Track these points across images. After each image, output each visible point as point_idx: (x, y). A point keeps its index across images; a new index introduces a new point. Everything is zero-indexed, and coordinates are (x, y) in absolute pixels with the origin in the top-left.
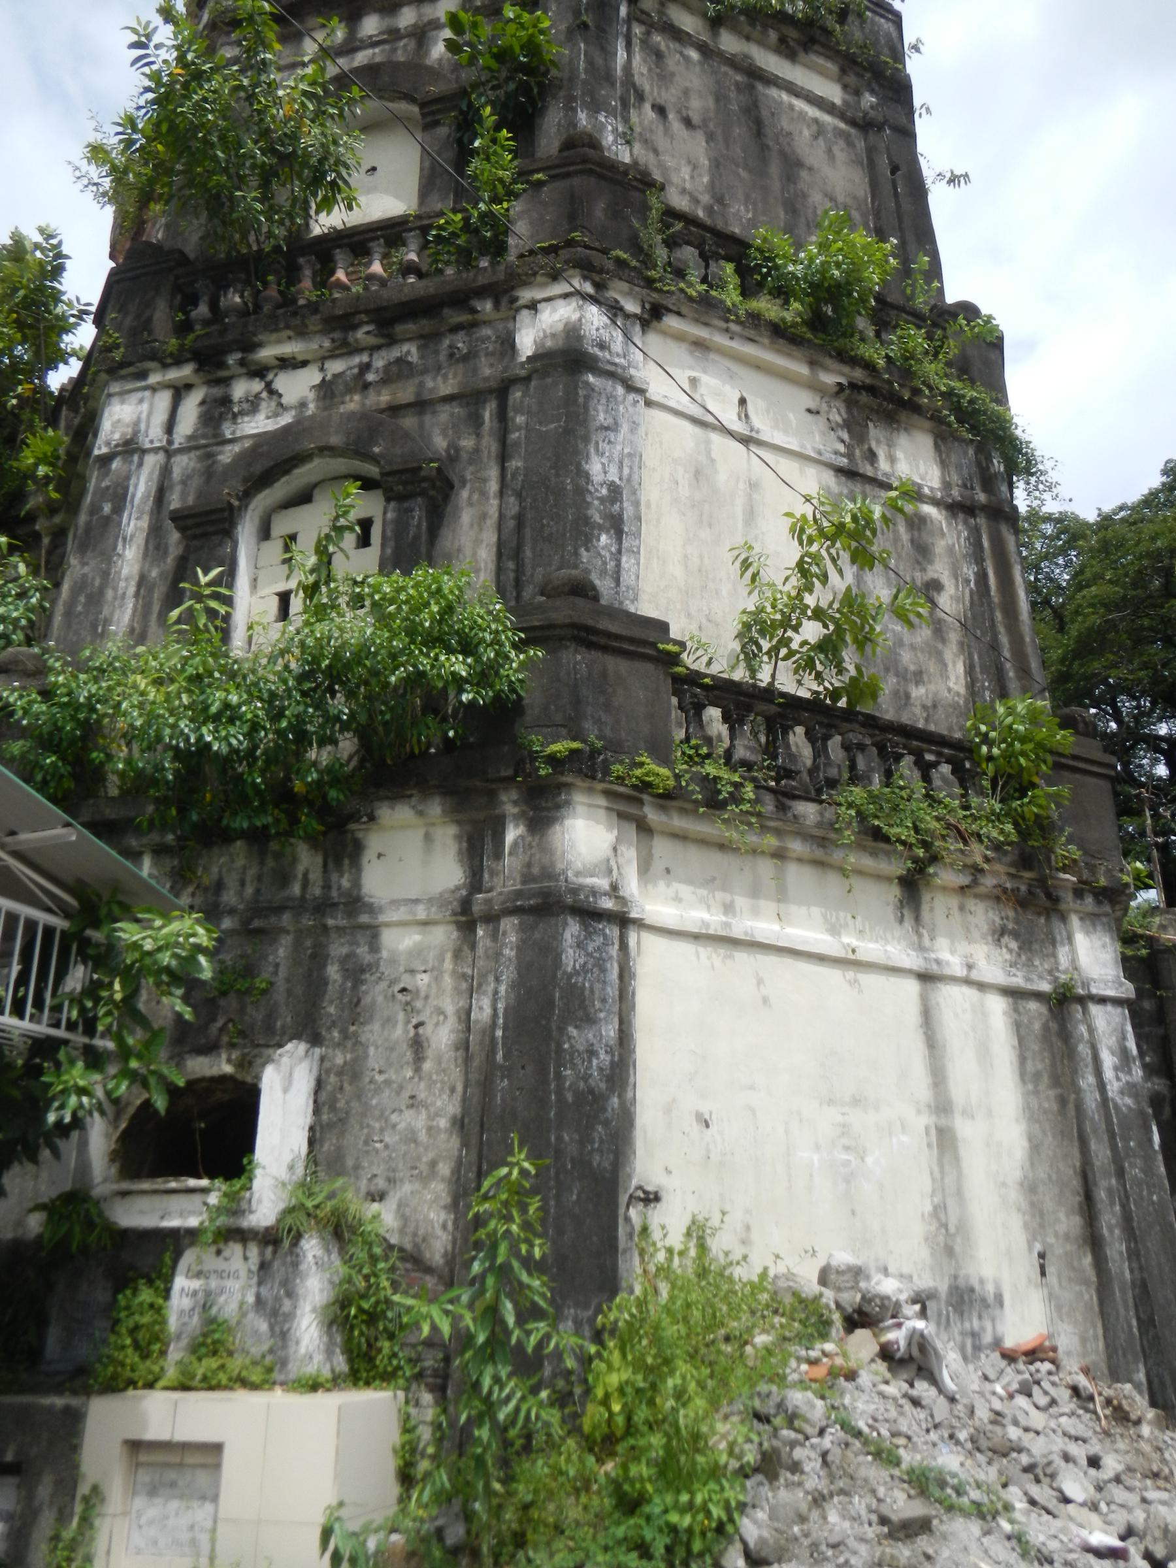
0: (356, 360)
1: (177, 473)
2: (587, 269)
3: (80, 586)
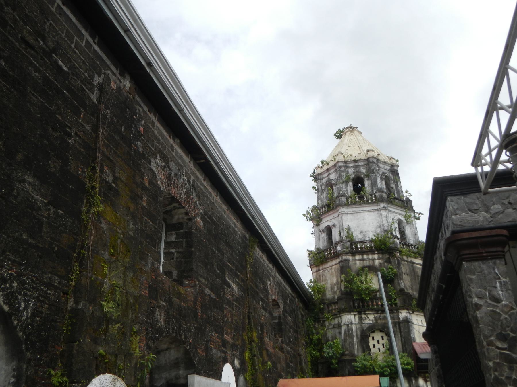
0: (379, 315)
1: (357, 327)
2: (408, 309)
3: (350, 343)
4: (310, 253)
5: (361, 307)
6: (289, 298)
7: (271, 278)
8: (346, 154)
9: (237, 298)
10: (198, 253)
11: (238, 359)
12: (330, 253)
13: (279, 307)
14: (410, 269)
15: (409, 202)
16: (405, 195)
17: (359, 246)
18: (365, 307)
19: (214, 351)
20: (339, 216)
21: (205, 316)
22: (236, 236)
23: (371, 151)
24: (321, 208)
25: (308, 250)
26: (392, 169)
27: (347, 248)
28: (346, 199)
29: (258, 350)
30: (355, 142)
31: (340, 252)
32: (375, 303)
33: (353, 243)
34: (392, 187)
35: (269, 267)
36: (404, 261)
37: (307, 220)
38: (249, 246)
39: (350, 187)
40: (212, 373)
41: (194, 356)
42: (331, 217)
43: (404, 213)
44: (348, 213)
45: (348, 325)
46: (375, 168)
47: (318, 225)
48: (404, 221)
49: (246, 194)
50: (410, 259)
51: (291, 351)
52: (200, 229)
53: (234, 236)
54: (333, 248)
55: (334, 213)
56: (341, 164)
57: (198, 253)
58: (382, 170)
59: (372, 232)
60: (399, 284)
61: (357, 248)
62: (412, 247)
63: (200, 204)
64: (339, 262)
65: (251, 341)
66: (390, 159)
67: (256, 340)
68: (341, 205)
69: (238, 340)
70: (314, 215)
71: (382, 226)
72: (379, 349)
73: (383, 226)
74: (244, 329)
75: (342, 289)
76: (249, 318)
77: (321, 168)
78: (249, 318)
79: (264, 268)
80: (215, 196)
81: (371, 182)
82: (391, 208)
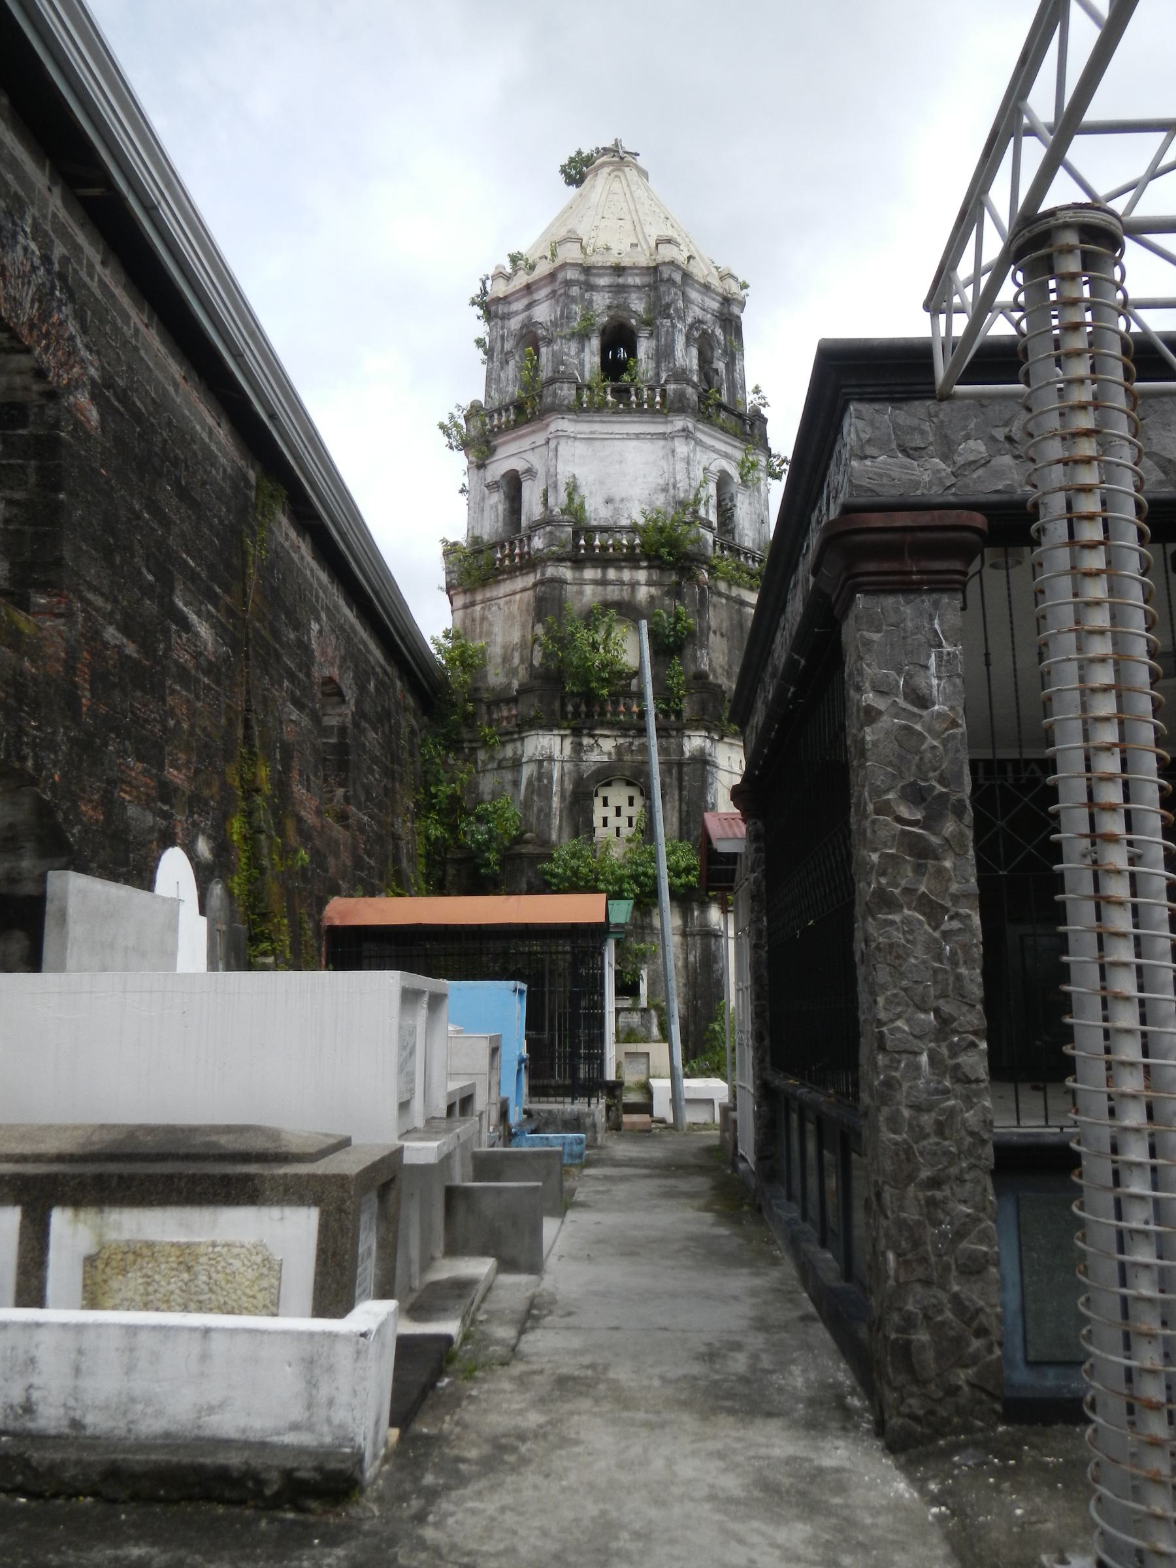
1: (566, 769)
2: (708, 730)
3: (540, 810)
4: (451, 550)
5: (583, 716)
6: (377, 679)
7: (324, 616)
8: (592, 241)
9: (210, 662)
10: (80, 512)
11: (209, 837)
12: (511, 556)
13: (343, 701)
14: (731, 619)
15: (757, 423)
16: (750, 397)
17: (597, 542)
18: (593, 716)
19: (132, 811)
20: (548, 441)
21: (103, 710)
22: (214, 472)
23: (669, 241)
24: (495, 411)
25: (444, 541)
26: (725, 310)
27: (564, 546)
28: (574, 392)
29: (270, 817)
30: (624, 205)
31: (539, 554)
32: (622, 708)
33: (583, 529)
34: (716, 370)
35: (318, 579)
36: (720, 594)
37: (451, 448)
38: (255, 507)
39: (593, 353)
40: (124, 870)
41: (66, 819)
42: (525, 443)
43: (739, 455)
44: (575, 438)
45: (540, 762)
46: (674, 301)
47: (481, 466)
48: (737, 479)
49: (252, 335)
50: (735, 592)
51: (370, 826)
52: (88, 436)
53: (205, 471)
54: (521, 541)
55: (534, 432)
56: (571, 274)
57: (80, 512)
58: (695, 312)
59: (641, 502)
60: (695, 659)
61: (590, 546)
62: (746, 558)
63: (87, 347)
64: (535, 585)
65: (251, 790)
66: (722, 278)
67: (267, 788)
68: (558, 409)
69: (208, 784)
70: (473, 433)
71: (671, 487)
72: (618, 829)
73: (674, 487)
74: (228, 756)
75: (536, 663)
76: (247, 725)
77: (508, 278)
78: (247, 725)
79: (300, 581)
80: (142, 328)
81: (657, 347)
82: (708, 436)
